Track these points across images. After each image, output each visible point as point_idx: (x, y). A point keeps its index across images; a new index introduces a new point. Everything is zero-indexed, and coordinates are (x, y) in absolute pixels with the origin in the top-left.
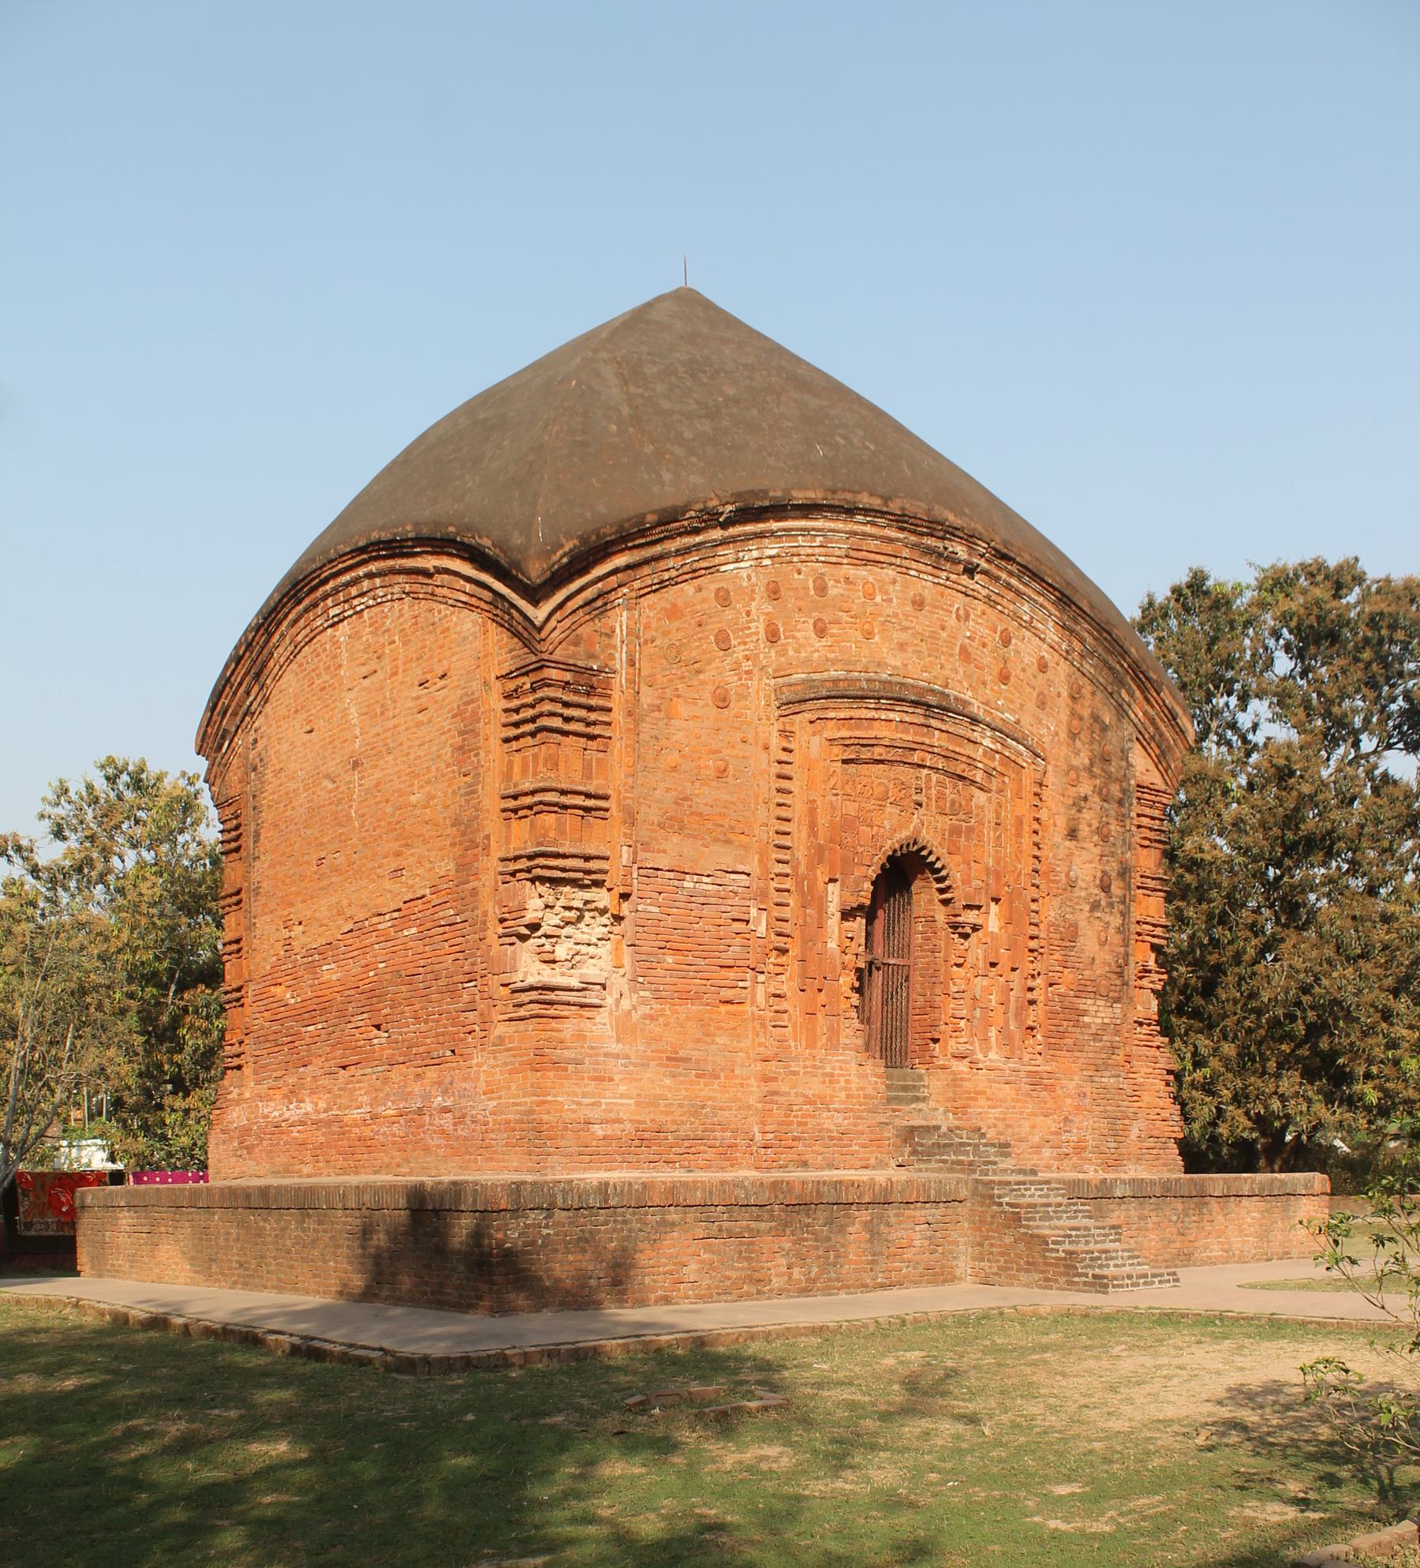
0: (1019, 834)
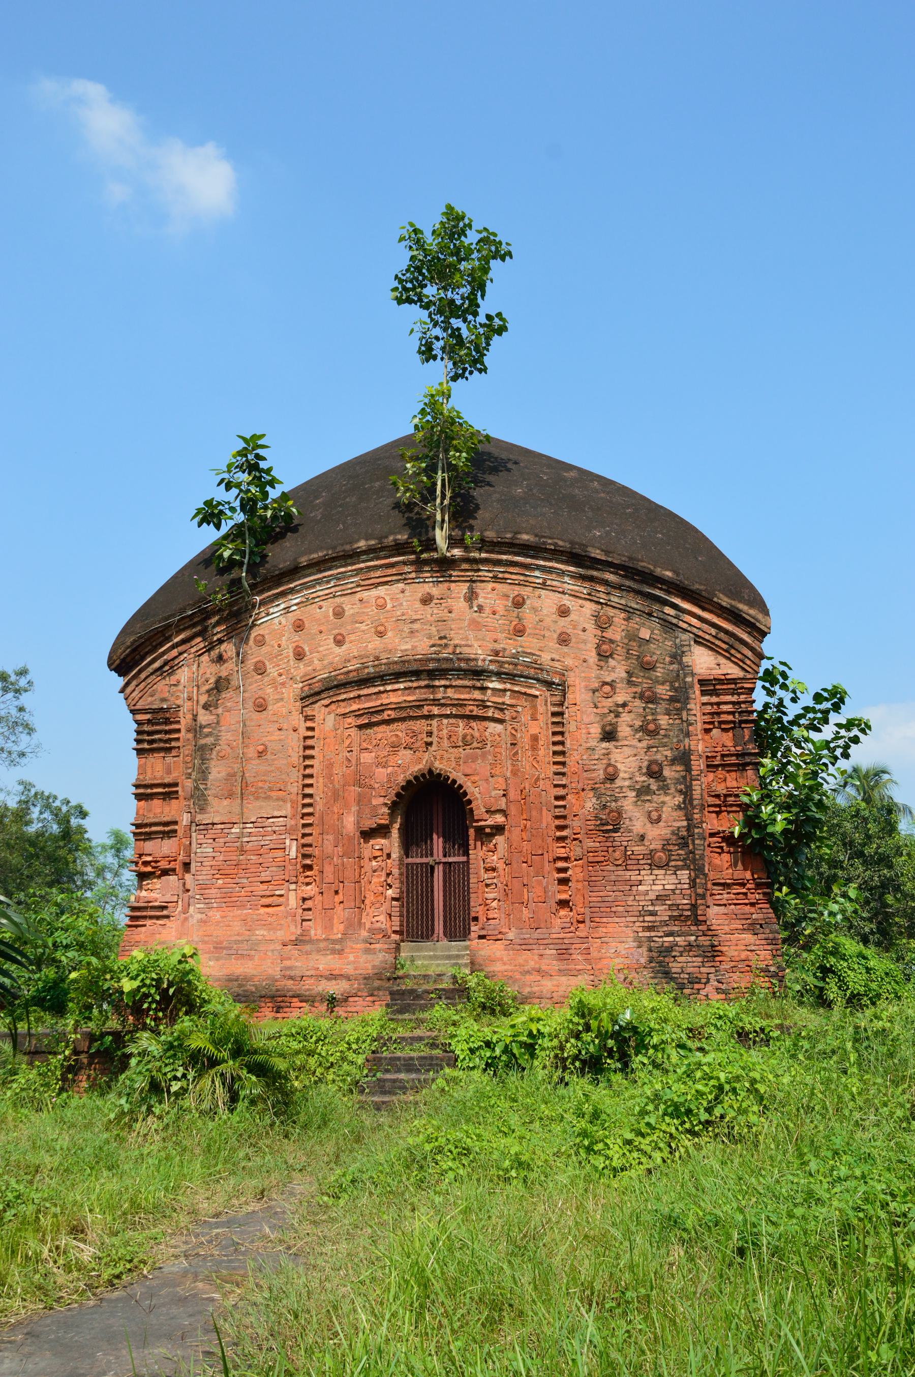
0: (534, 748)
